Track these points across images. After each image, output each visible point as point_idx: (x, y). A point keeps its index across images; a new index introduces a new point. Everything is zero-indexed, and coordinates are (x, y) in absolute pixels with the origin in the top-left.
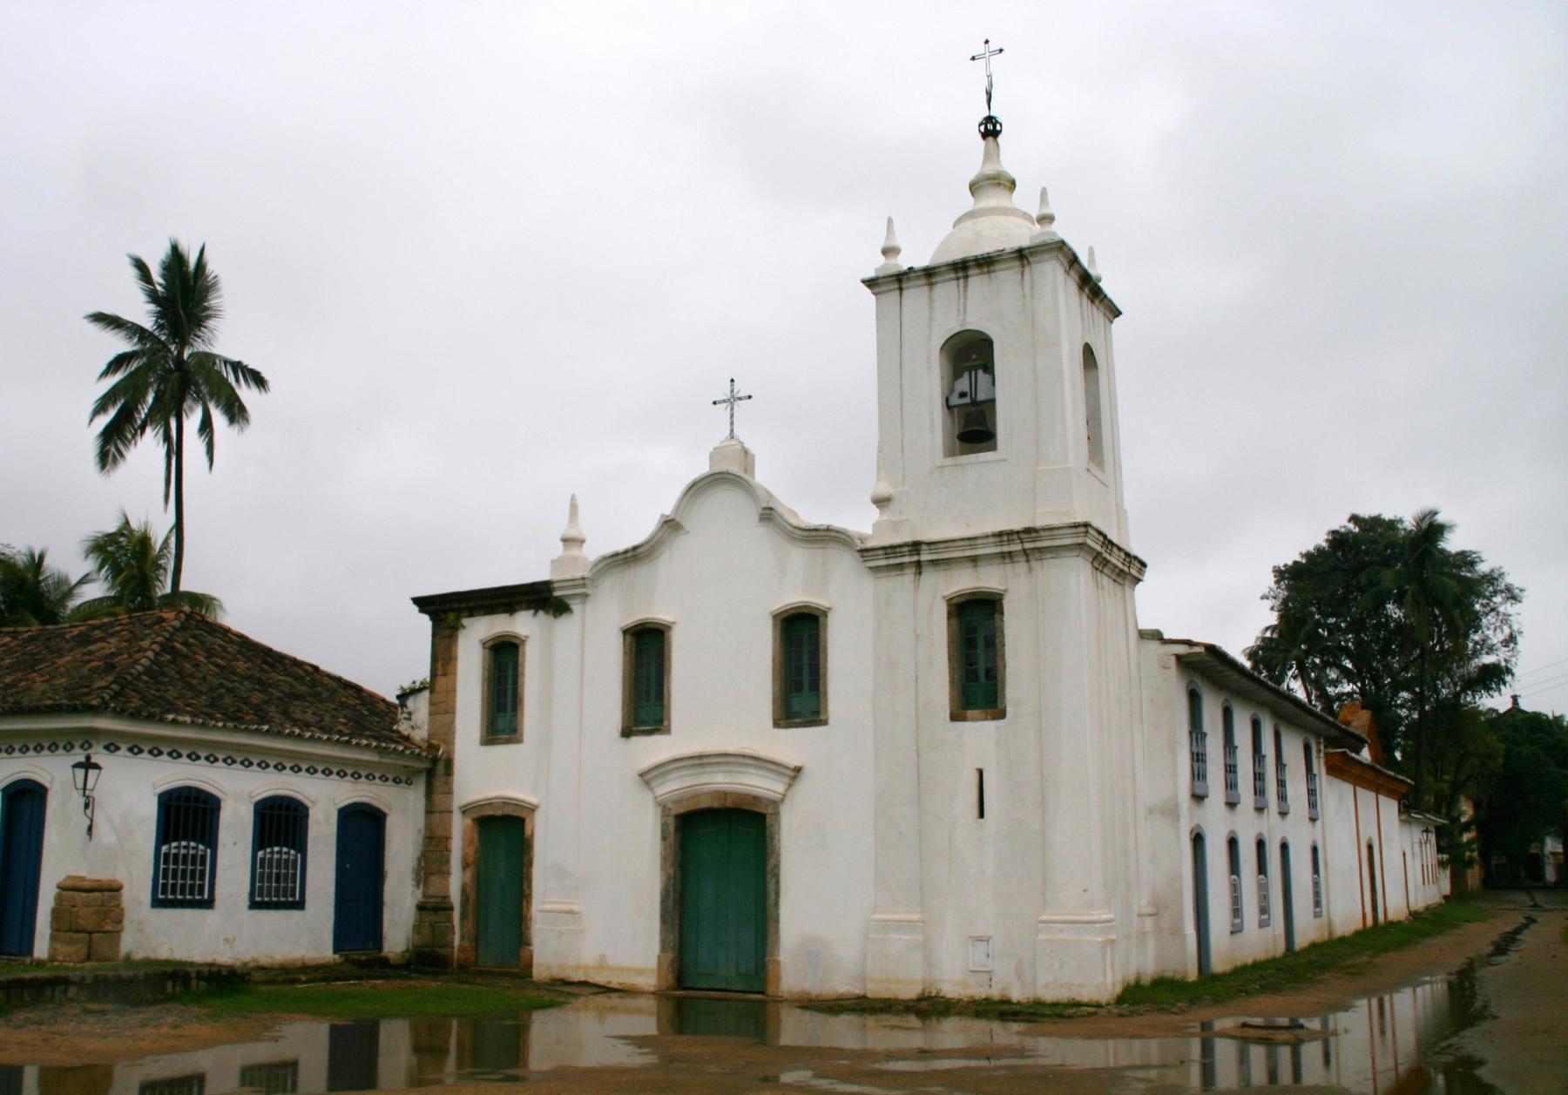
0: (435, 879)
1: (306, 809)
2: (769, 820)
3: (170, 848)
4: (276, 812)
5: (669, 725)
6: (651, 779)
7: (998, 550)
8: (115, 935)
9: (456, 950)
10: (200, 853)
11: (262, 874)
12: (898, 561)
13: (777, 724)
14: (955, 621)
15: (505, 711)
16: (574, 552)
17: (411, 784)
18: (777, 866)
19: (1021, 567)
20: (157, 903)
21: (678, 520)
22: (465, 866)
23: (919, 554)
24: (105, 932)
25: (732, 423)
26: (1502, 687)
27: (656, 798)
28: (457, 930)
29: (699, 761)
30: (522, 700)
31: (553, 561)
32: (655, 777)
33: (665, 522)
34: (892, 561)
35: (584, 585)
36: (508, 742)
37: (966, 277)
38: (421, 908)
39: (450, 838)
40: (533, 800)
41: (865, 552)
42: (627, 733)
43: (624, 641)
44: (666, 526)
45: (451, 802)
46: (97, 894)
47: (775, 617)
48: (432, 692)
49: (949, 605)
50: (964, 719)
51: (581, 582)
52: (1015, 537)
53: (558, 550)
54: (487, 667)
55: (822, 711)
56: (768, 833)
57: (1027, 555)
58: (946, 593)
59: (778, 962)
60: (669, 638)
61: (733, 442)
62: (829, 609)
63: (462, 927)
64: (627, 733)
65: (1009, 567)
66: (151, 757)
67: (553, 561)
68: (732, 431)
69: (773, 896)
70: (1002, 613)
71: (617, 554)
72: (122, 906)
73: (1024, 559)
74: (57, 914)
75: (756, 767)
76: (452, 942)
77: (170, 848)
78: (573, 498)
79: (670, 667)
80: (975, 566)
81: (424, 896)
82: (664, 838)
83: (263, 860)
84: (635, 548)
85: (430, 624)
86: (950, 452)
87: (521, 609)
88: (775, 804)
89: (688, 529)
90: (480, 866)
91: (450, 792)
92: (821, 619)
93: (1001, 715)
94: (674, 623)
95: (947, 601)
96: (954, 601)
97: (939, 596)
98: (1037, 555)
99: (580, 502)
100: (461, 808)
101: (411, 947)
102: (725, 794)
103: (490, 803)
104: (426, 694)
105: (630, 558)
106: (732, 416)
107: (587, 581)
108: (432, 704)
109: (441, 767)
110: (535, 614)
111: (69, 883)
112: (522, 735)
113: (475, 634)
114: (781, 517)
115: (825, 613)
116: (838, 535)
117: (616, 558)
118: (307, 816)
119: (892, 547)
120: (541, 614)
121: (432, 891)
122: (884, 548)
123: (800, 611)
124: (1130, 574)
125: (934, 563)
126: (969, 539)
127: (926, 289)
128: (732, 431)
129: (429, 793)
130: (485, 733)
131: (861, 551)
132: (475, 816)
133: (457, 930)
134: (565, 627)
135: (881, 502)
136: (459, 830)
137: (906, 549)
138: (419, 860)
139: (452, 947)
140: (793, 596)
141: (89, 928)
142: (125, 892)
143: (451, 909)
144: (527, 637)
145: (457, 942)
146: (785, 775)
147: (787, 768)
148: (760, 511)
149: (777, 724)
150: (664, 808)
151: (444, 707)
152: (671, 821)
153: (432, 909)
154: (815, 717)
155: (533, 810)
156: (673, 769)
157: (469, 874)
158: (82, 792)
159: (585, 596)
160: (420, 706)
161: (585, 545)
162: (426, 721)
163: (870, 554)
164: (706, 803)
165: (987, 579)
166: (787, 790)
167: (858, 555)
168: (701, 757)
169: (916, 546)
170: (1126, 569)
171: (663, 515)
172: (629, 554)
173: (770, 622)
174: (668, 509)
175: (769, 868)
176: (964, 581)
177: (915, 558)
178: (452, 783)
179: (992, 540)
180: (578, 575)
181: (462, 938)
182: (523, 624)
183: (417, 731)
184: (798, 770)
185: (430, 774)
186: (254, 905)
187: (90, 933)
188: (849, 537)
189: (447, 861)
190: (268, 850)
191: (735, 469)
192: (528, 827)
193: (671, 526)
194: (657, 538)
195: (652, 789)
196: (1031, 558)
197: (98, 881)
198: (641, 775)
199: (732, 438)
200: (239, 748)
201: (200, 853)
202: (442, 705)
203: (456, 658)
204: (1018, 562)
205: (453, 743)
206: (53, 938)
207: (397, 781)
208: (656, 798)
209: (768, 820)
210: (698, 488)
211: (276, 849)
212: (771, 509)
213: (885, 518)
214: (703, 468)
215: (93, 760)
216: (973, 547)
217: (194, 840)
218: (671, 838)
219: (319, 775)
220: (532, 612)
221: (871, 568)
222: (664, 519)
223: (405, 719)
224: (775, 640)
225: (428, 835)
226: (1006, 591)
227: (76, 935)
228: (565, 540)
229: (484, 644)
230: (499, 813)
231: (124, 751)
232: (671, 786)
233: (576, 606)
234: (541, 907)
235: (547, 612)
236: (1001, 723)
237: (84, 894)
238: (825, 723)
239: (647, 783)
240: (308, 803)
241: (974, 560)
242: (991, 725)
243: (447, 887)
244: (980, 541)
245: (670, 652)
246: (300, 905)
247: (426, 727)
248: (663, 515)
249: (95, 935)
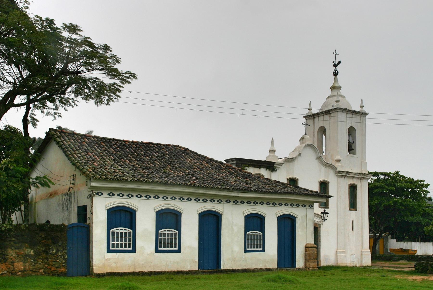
2: (319, 228)
7: (358, 176)
18: (320, 239)
37: (352, 114)
49: (349, 186)
50: (351, 210)
56: (318, 232)
59: (321, 261)
66: (241, 204)
69: (319, 246)
78: (272, 139)
88: (320, 225)
93: (356, 210)
96: (350, 185)
105: (289, 160)
106: (306, 129)
110: (266, 169)
117: (288, 160)
120: (267, 170)
122: (342, 172)
123: (324, 182)
126: (355, 173)
127: (346, 114)
128: (306, 133)
140: (322, 179)
148: (318, 156)
175: (319, 240)
179: (358, 174)
216: (355, 175)
220: (265, 169)
224: (319, 187)
235: (269, 170)
236: (356, 212)
242: (355, 212)
244: (356, 174)
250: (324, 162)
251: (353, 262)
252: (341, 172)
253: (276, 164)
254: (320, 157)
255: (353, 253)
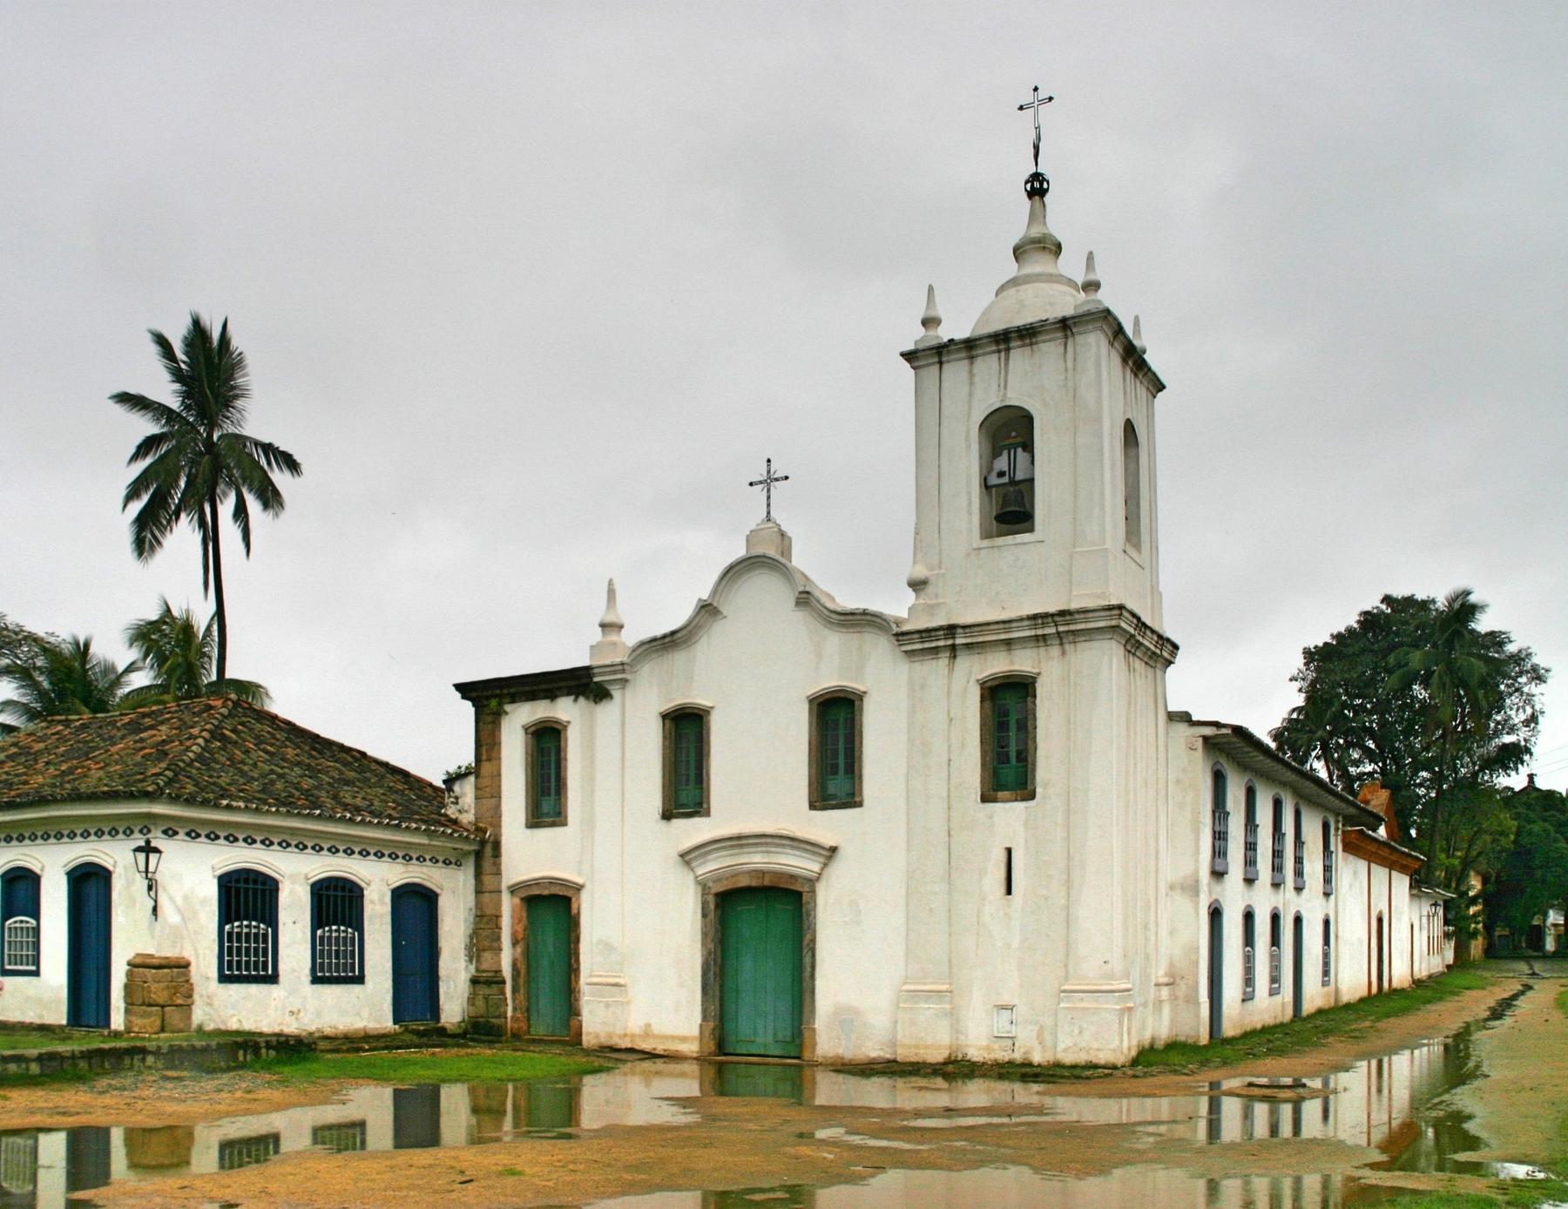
0: (487, 955)
1: (361, 890)
3: (233, 927)
4: (332, 893)
5: (709, 808)
6: (691, 859)
7: (1033, 633)
8: (187, 1008)
9: (509, 1020)
10: (261, 932)
11: (322, 951)
12: (933, 644)
13: (812, 807)
14: (988, 704)
15: (549, 795)
16: (613, 637)
17: (460, 865)
19: (1055, 651)
20: (224, 979)
21: (715, 604)
22: (515, 943)
23: (954, 638)
24: (177, 1006)
25: (769, 505)
26: (1520, 766)
27: (696, 877)
28: (509, 1001)
29: (738, 841)
30: (565, 785)
31: (592, 647)
32: (695, 858)
33: (703, 607)
34: (927, 645)
35: (623, 671)
36: (553, 825)
38: (475, 981)
39: (501, 916)
40: (580, 880)
41: (901, 636)
42: (667, 816)
43: (664, 726)
44: (703, 611)
45: (500, 882)
46: (166, 971)
47: (811, 701)
48: (477, 778)
49: (982, 689)
51: (620, 667)
52: (1050, 620)
53: (597, 635)
54: (530, 752)
55: (857, 793)
57: (1061, 639)
58: (980, 677)
60: (708, 722)
61: (770, 525)
62: (865, 693)
63: (514, 1000)
64: (667, 816)
65: (1042, 650)
67: (592, 647)
68: (769, 513)
70: (1035, 696)
71: (654, 640)
72: (191, 981)
73: (1058, 642)
74: (128, 988)
75: (793, 847)
76: (506, 1013)
77: (233, 927)
78: (610, 583)
79: (709, 751)
80: (1009, 650)
81: (477, 970)
82: (704, 915)
83: (322, 938)
84: (673, 633)
85: (473, 710)
86: (986, 535)
87: (562, 695)
88: (812, 882)
89: (725, 613)
90: (527, 942)
91: (498, 873)
92: (857, 703)
94: (712, 708)
95: (981, 684)
96: (988, 684)
97: (973, 680)
98: (1071, 638)
99: (617, 586)
100: (509, 888)
101: (466, 1018)
102: (763, 873)
103: (537, 882)
104: (472, 779)
105: (668, 642)
106: (769, 498)
107: (626, 667)
108: (477, 788)
109: (488, 850)
110: (576, 700)
111: (138, 961)
112: (566, 817)
113: (517, 720)
114: (818, 601)
115: (860, 696)
116: (874, 619)
117: (654, 644)
118: (362, 896)
119: (928, 631)
120: (582, 700)
121: (485, 966)
122: (919, 632)
124: (1162, 656)
125: (968, 646)
126: (1004, 622)
128: (769, 513)
129: (478, 875)
130: (530, 817)
131: (897, 635)
132: (523, 896)
133: (509, 1001)
134: (606, 713)
135: (917, 585)
136: (508, 907)
137: (941, 633)
138: (471, 937)
139: (506, 1018)
140: (829, 680)
141: (161, 1001)
142: (193, 968)
143: (504, 982)
144: (569, 722)
145: (509, 1014)
146: (820, 854)
147: (823, 848)
148: (797, 594)
149: (812, 807)
150: (703, 886)
151: (490, 793)
152: (711, 899)
153: (484, 982)
154: (851, 799)
155: (579, 890)
156: (715, 849)
157: (519, 950)
158: (144, 875)
159: (626, 681)
160: (466, 790)
161: (623, 630)
162: (473, 805)
163: (905, 638)
164: (744, 882)
165: (1022, 662)
166: (822, 869)
167: (893, 639)
168: (739, 838)
169: (951, 630)
170: (1158, 651)
171: (700, 600)
172: (667, 640)
173: (806, 706)
174: (705, 595)
176: (998, 664)
177: (950, 642)
178: (500, 864)
180: (618, 660)
181: (515, 1009)
182: (564, 709)
183: (465, 815)
184: (834, 850)
185: (479, 856)
186: (316, 980)
187: (163, 1007)
188: (885, 620)
189: (498, 938)
190: (327, 929)
191: (772, 552)
192: (574, 906)
193: (707, 610)
194: (693, 624)
195: (692, 870)
196: (1065, 641)
197: (167, 958)
198: (682, 856)
199: (769, 520)
200: (294, 831)
201: (261, 932)
202: (487, 789)
203: (500, 744)
204: (1052, 645)
205: (500, 826)
206: (127, 1011)
207: (447, 863)
208: (696, 877)
209: (804, 897)
210: (734, 572)
211: (334, 927)
212: (808, 593)
213: (922, 601)
214: (741, 552)
215: (154, 844)
217: (255, 920)
218: (712, 916)
219: (372, 857)
220: (572, 697)
221: (906, 652)
222: (701, 604)
223: (452, 803)
224: (810, 723)
225: (479, 914)
226: (1039, 674)
227: (149, 1009)
228: (603, 626)
229: (526, 729)
230: (546, 892)
231: (181, 836)
232: (712, 865)
233: (616, 694)
234: (589, 981)
235: (587, 698)
237: (154, 971)
238: (860, 804)
239: (688, 863)
240: (363, 885)
241: (1008, 643)
243: (499, 963)
244: (1014, 625)
245: (709, 737)
246: (360, 980)
247: (473, 811)
248: (700, 600)
249: (167, 1009)
250: (827, 613)
251: (1010, 1042)
252: (916, 636)
253: (595, 671)
254: (805, 596)
255: (1006, 999)
